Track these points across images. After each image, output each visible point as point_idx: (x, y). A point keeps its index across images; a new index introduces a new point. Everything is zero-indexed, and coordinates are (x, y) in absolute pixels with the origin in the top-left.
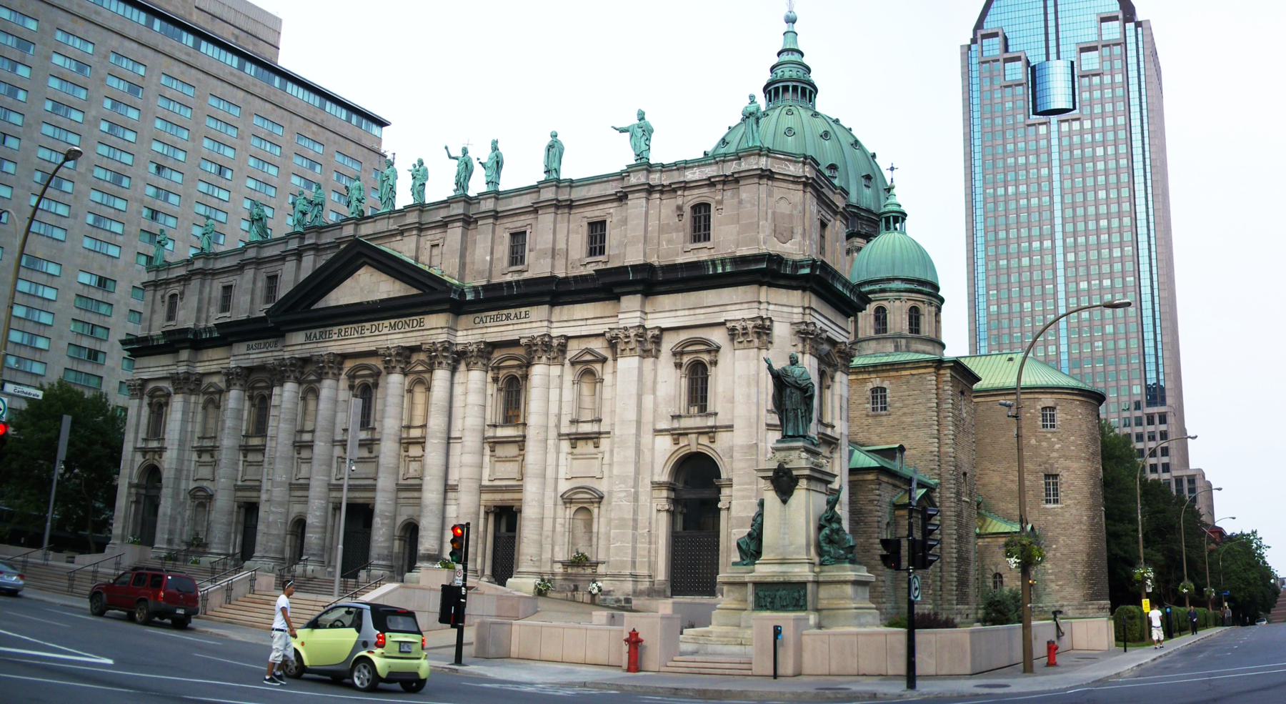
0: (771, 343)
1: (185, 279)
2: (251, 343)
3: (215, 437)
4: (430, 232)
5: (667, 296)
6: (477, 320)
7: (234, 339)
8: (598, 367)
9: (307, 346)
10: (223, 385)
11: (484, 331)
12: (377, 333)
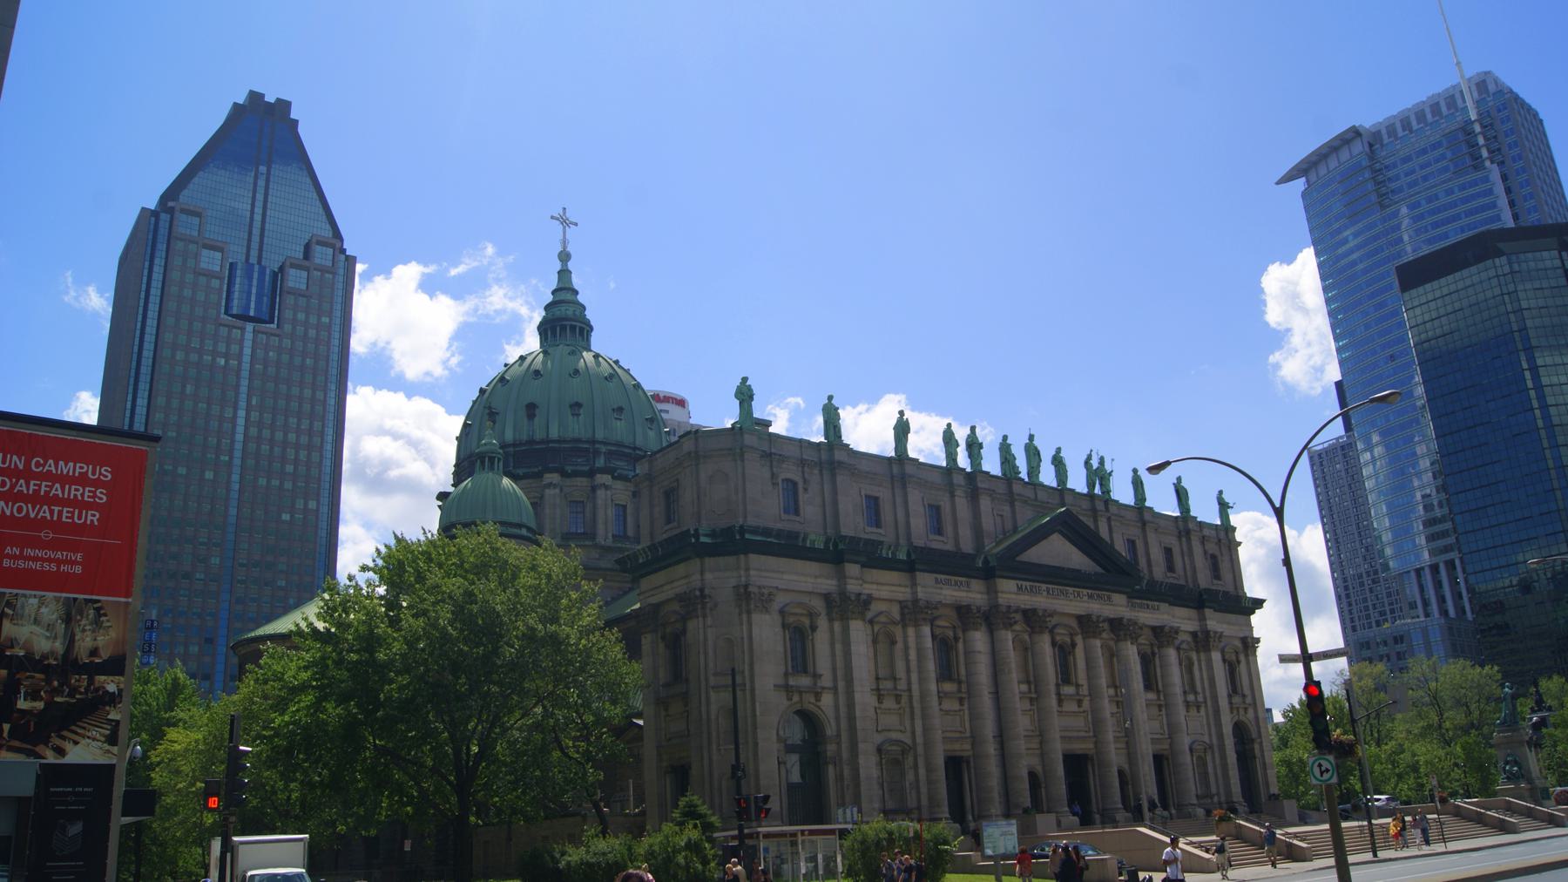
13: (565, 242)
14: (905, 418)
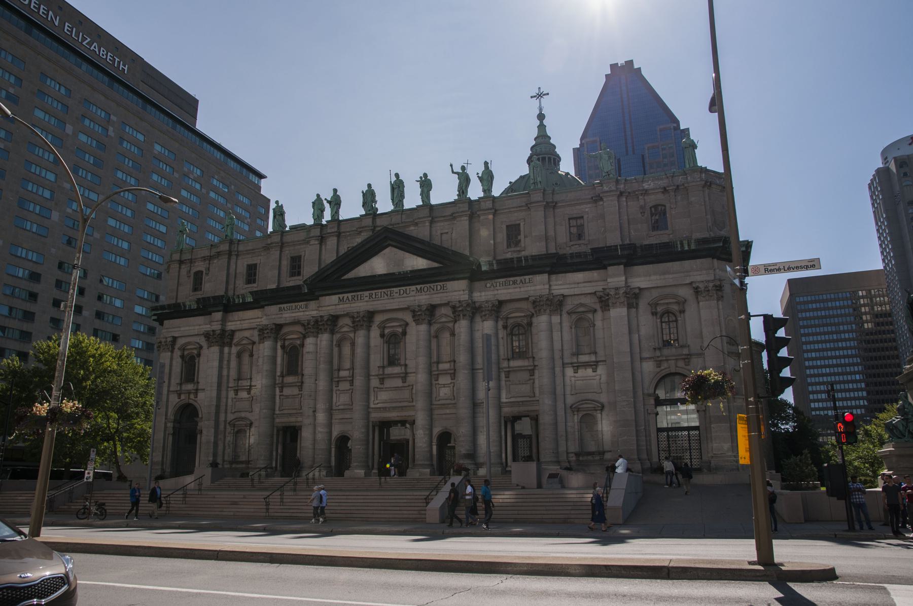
0: (722, 297)
1: (210, 258)
2: (282, 306)
3: (251, 379)
4: (439, 224)
5: (640, 266)
6: (488, 285)
7: (267, 303)
8: (590, 316)
9: (341, 306)
10: (256, 339)
11: (496, 292)
12: (405, 295)
13: (541, 109)
14: (280, 205)
